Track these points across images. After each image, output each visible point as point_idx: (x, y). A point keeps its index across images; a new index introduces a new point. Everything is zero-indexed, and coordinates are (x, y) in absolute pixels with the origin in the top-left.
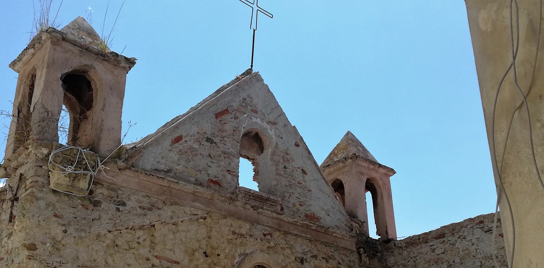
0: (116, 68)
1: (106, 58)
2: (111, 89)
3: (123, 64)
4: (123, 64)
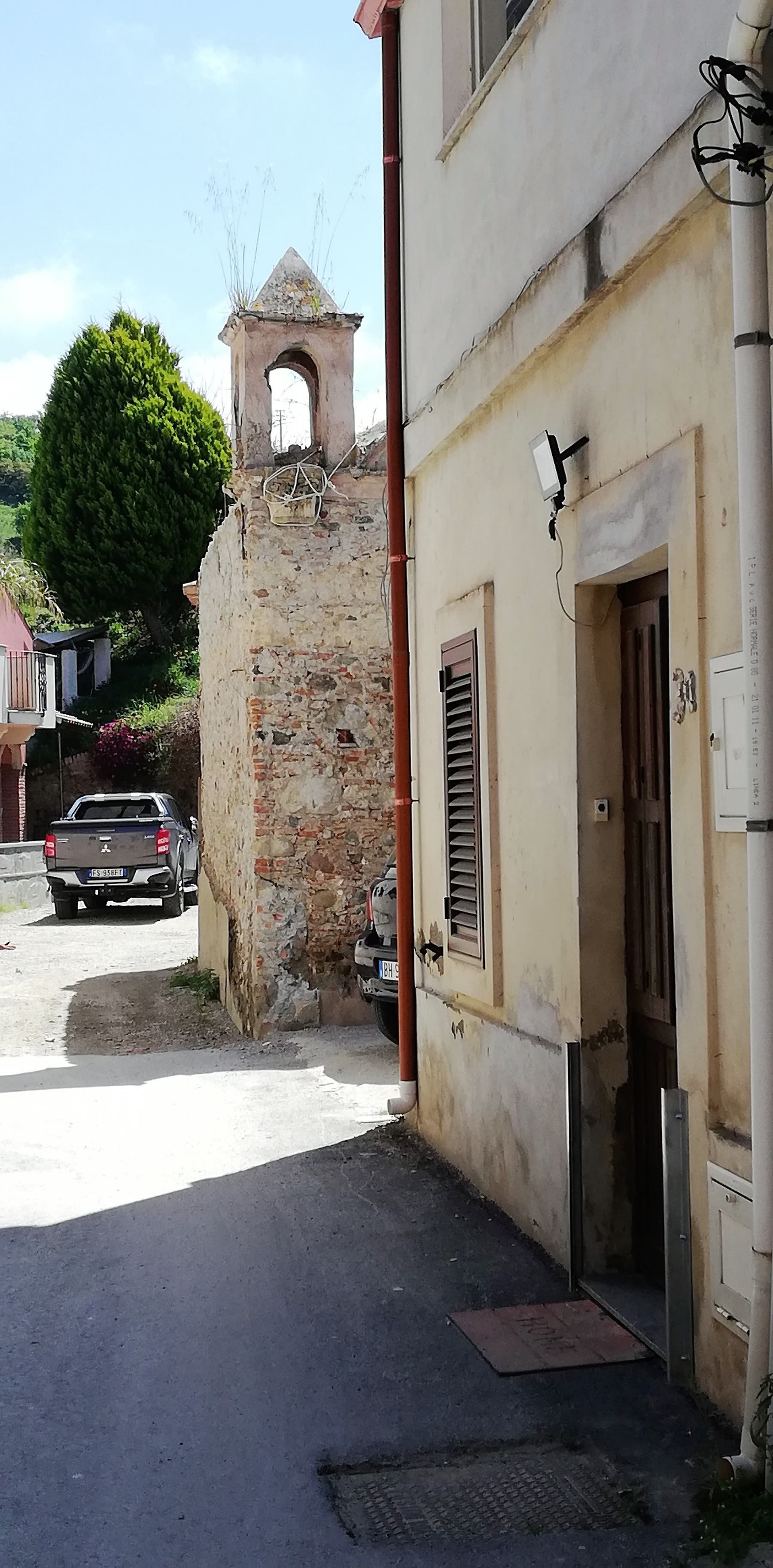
0: (337, 333)
1: (321, 324)
2: (334, 366)
3: (345, 325)
4: (345, 325)
